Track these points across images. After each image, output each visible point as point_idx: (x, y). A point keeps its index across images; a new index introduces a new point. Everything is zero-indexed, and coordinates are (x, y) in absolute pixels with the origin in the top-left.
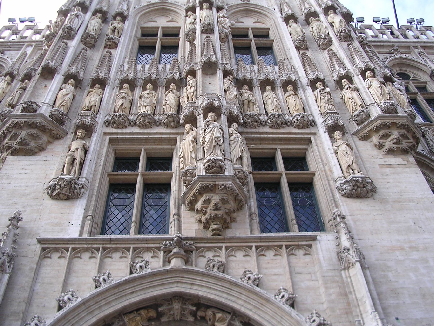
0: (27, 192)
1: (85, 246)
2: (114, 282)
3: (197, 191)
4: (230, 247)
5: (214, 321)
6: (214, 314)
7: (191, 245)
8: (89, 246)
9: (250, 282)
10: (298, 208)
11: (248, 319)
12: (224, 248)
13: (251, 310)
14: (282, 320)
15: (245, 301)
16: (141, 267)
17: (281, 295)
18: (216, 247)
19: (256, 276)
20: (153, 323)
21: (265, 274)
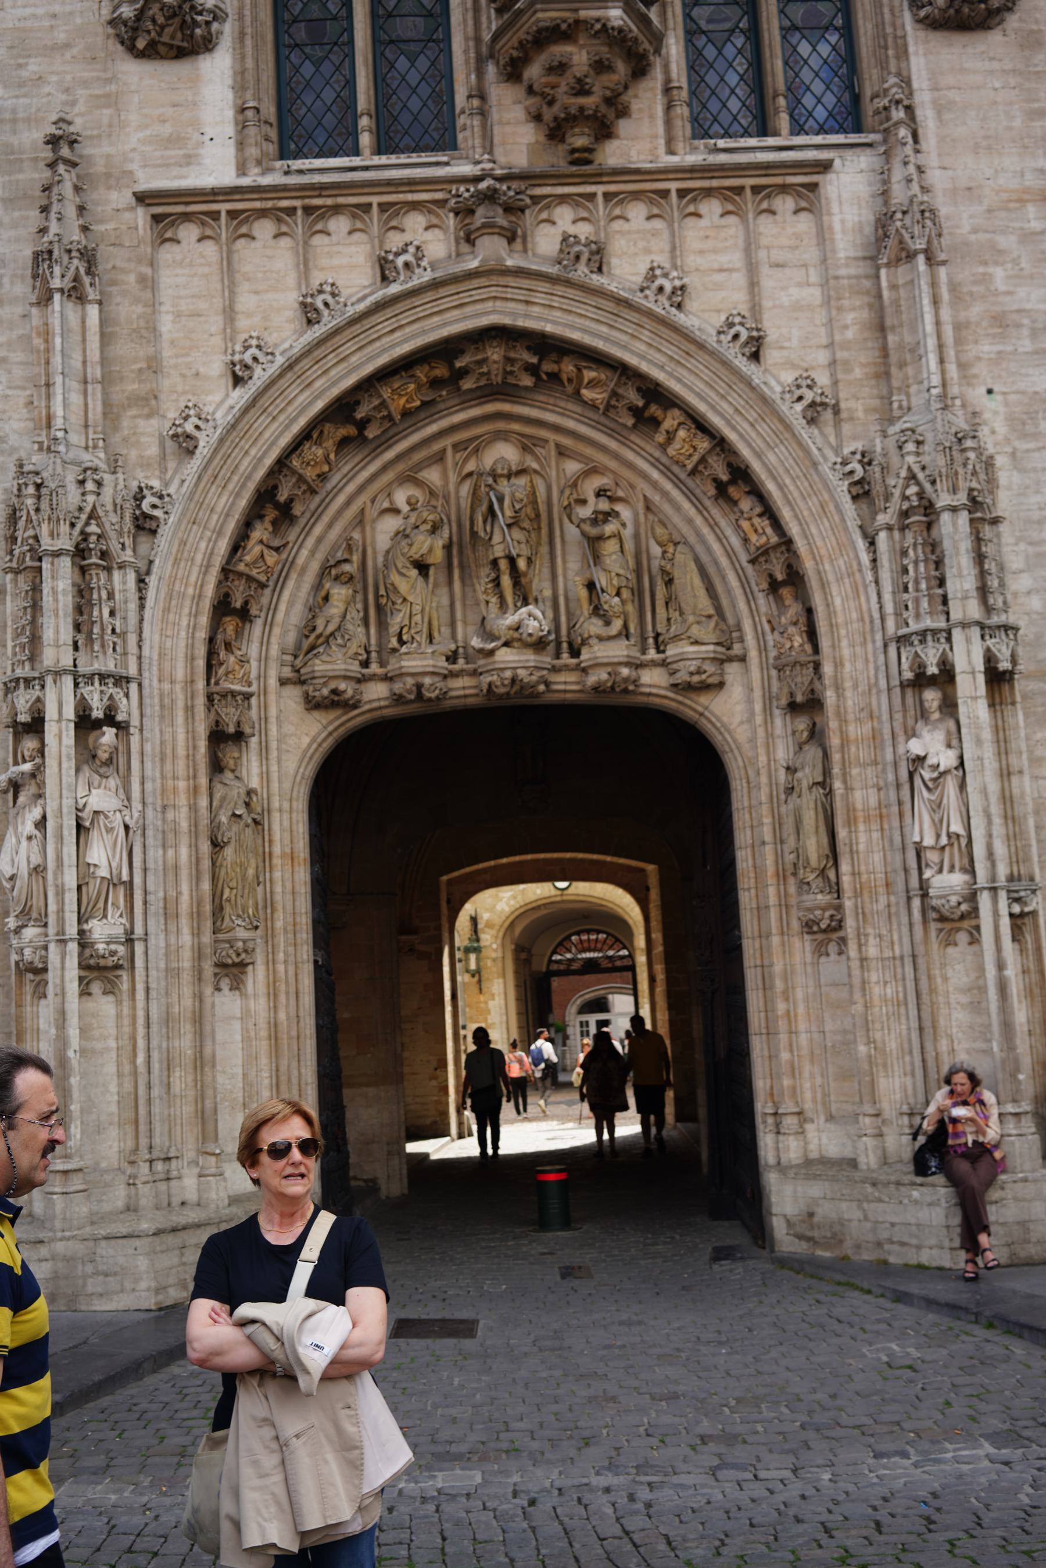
0: (61, 36)
1: (258, 205)
2: (350, 311)
3: (530, 38)
4: (616, 194)
6: (579, 370)
7: (517, 193)
9: (663, 299)
10: (796, 37)
12: (600, 199)
13: (662, 368)
15: (650, 345)
16: (407, 265)
17: (733, 332)
18: (580, 195)
19: (678, 283)
20: (444, 393)
21: (697, 270)
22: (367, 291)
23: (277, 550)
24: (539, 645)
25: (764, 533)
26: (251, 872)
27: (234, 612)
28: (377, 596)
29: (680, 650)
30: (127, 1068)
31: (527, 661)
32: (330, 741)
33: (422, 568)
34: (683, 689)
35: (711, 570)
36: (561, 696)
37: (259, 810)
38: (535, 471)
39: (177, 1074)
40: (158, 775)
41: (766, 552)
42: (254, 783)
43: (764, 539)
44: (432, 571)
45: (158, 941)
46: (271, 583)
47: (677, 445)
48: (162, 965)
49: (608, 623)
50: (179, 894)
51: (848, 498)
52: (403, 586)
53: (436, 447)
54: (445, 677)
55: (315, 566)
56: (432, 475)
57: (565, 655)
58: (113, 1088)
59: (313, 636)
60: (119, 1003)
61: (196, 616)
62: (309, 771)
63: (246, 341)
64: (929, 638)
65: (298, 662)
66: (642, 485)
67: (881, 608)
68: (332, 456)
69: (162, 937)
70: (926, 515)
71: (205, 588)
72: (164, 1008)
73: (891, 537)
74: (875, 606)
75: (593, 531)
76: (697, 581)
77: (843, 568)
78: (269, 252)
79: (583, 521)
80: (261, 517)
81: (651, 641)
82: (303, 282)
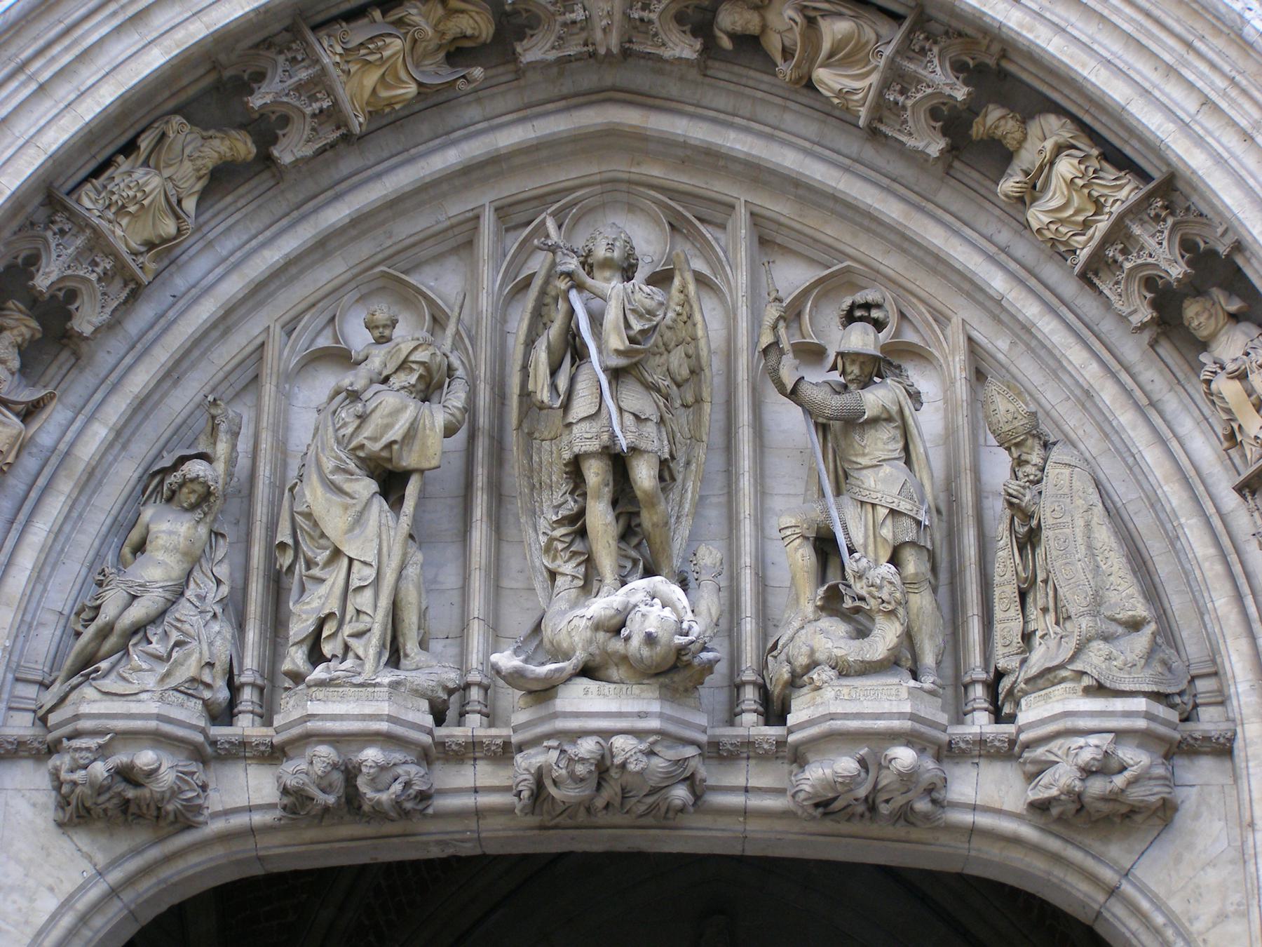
5: (811, 58)
6: (811, 22)
11: (996, 48)
14: (1191, 57)
20: (478, 72)
29: (1057, 708)
31: (641, 715)
32: (115, 911)
34: (1060, 819)
35: (1142, 522)
36: (735, 826)
44: (412, 489)
47: (1054, 198)
52: (334, 521)
53: (456, 208)
55: (126, 472)
57: (749, 718)
65: (49, 698)
66: (963, 312)
76: (1104, 535)
81: (979, 691)
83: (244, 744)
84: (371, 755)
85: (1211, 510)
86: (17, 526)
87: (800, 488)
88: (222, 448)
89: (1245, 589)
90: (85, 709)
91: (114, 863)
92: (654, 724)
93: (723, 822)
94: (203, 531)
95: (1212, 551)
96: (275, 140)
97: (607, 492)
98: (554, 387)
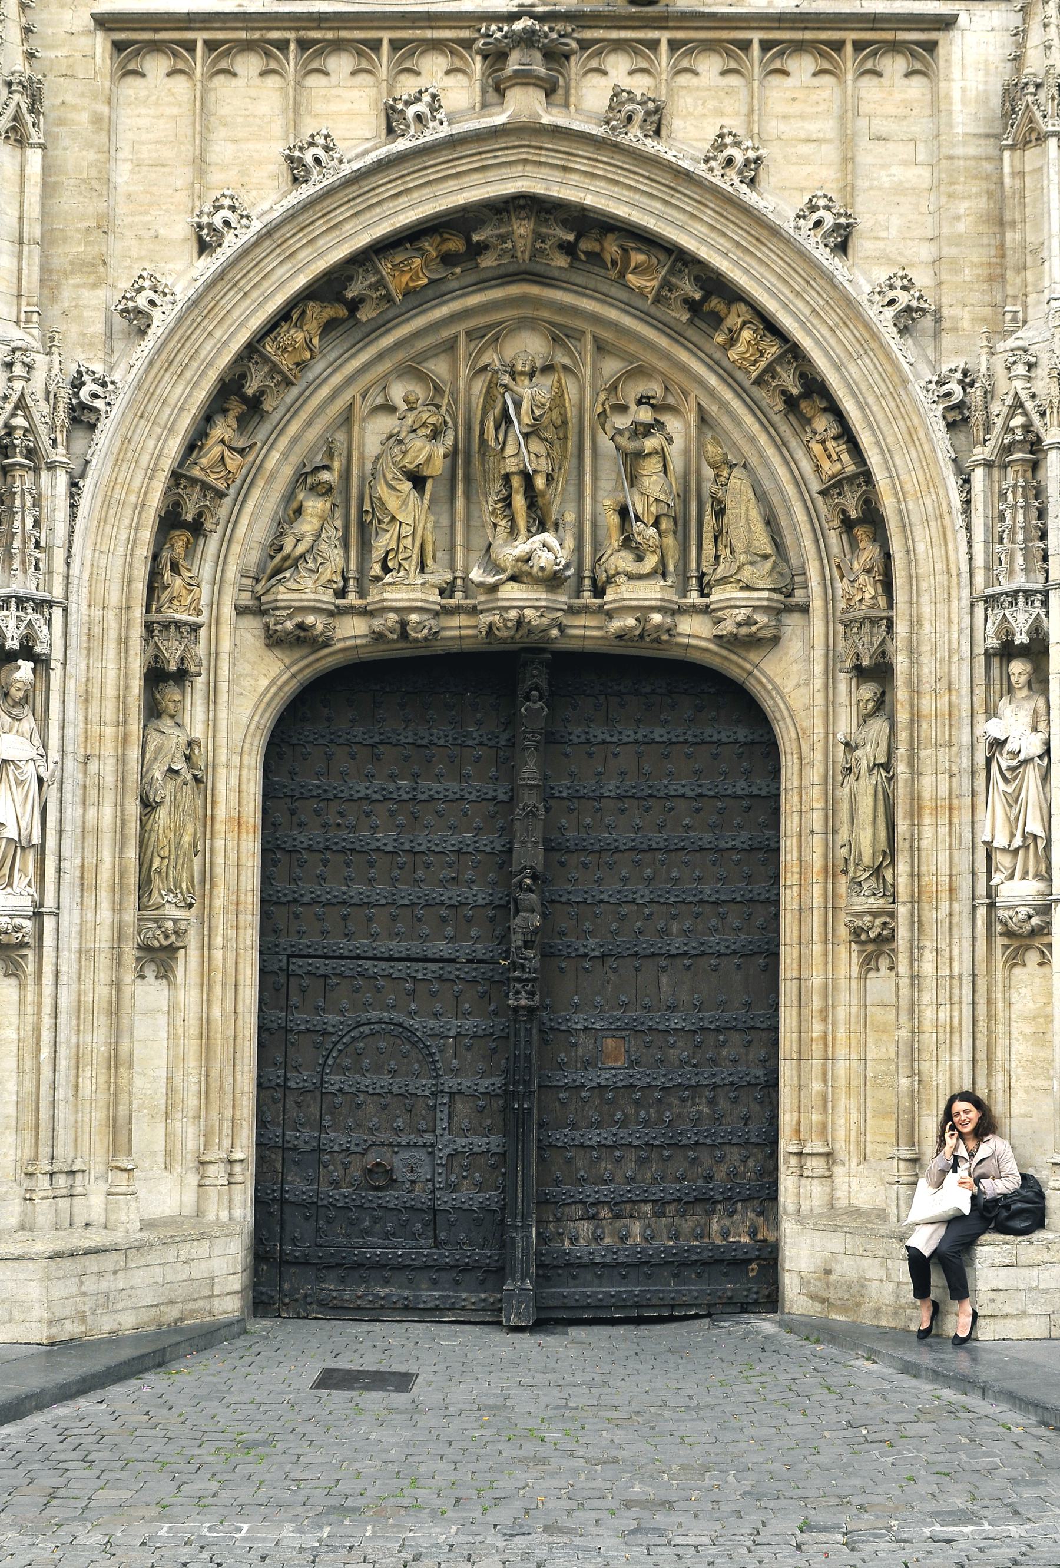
2: (347, 169)
8: (257, 35)
20: (458, 270)
22: (369, 145)
23: (241, 452)
24: (553, 581)
25: (839, 459)
26: (187, 839)
27: (183, 525)
28: (361, 513)
29: (728, 596)
30: (28, 1064)
33: (418, 481)
37: (202, 764)
38: (565, 368)
39: (88, 1074)
40: (81, 718)
41: (839, 485)
42: (198, 733)
43: (839, 466)
45: (70, 917)
46: (232, 491)
48: (75, 945)
49: (640, 559)
50: (99, 861)
51: (943, 423)
52: (392, 503)
53: (446, 333)
54: (437, 614)
55: (288, 472)
56: (439, 368)
57: (586, 594)
58: (11, 1086)
59: (279, 557)
60: (22, 986)
61: (137, 529)
62: (267, 719)
63: (217, 199)
64: (1021, 600)
65: (260, 588)
66: (695, 392)
67: (971, 559)
68: (315, 341)
69: (77, 911)
70: (1031, 453)
71: (149, 496)
72: (74, 996)
73: (989, 476)
74: (964, 558)
75: (631, 446)
77: (930, 509)
78: (253, 92)
79: (620, 432)
80: (225, 411)
82: (291, 131)
83: (352, 607)
84: (414, 617)
85: (807, 497)
86: (238, 503)
87: (614, 476)
88: (336, 465)
89: (820, 536)
90: (280, 597)
91: (294, 663)
92: (544, 604)
93: (573, 641)
94: (328, 505)
95: (806, 518)
96: (357, 309)
97: (522, 490)
98: (497, 438)
